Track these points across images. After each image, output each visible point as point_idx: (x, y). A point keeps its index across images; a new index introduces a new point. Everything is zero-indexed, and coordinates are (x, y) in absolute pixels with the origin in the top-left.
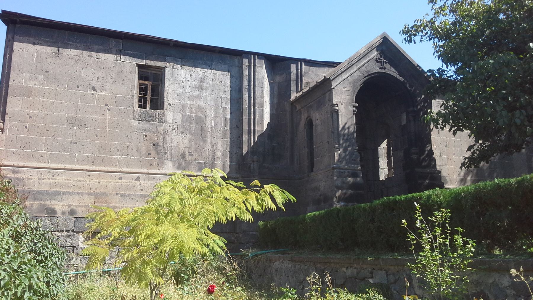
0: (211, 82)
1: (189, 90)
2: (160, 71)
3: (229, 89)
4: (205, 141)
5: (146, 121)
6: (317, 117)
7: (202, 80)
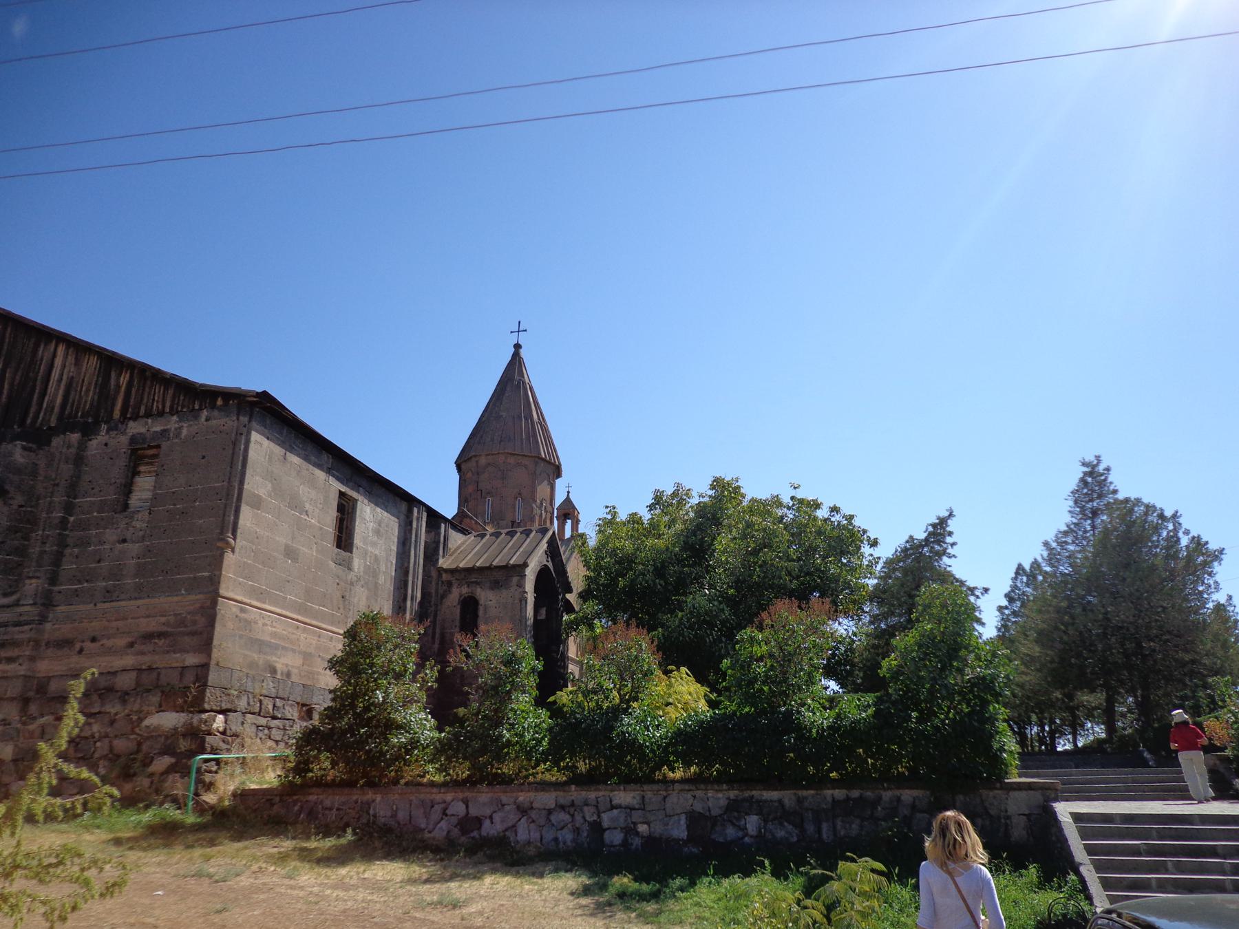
1: (370, 535)
3: (396, 540)
6: (487, 598)
7: (380, 525)
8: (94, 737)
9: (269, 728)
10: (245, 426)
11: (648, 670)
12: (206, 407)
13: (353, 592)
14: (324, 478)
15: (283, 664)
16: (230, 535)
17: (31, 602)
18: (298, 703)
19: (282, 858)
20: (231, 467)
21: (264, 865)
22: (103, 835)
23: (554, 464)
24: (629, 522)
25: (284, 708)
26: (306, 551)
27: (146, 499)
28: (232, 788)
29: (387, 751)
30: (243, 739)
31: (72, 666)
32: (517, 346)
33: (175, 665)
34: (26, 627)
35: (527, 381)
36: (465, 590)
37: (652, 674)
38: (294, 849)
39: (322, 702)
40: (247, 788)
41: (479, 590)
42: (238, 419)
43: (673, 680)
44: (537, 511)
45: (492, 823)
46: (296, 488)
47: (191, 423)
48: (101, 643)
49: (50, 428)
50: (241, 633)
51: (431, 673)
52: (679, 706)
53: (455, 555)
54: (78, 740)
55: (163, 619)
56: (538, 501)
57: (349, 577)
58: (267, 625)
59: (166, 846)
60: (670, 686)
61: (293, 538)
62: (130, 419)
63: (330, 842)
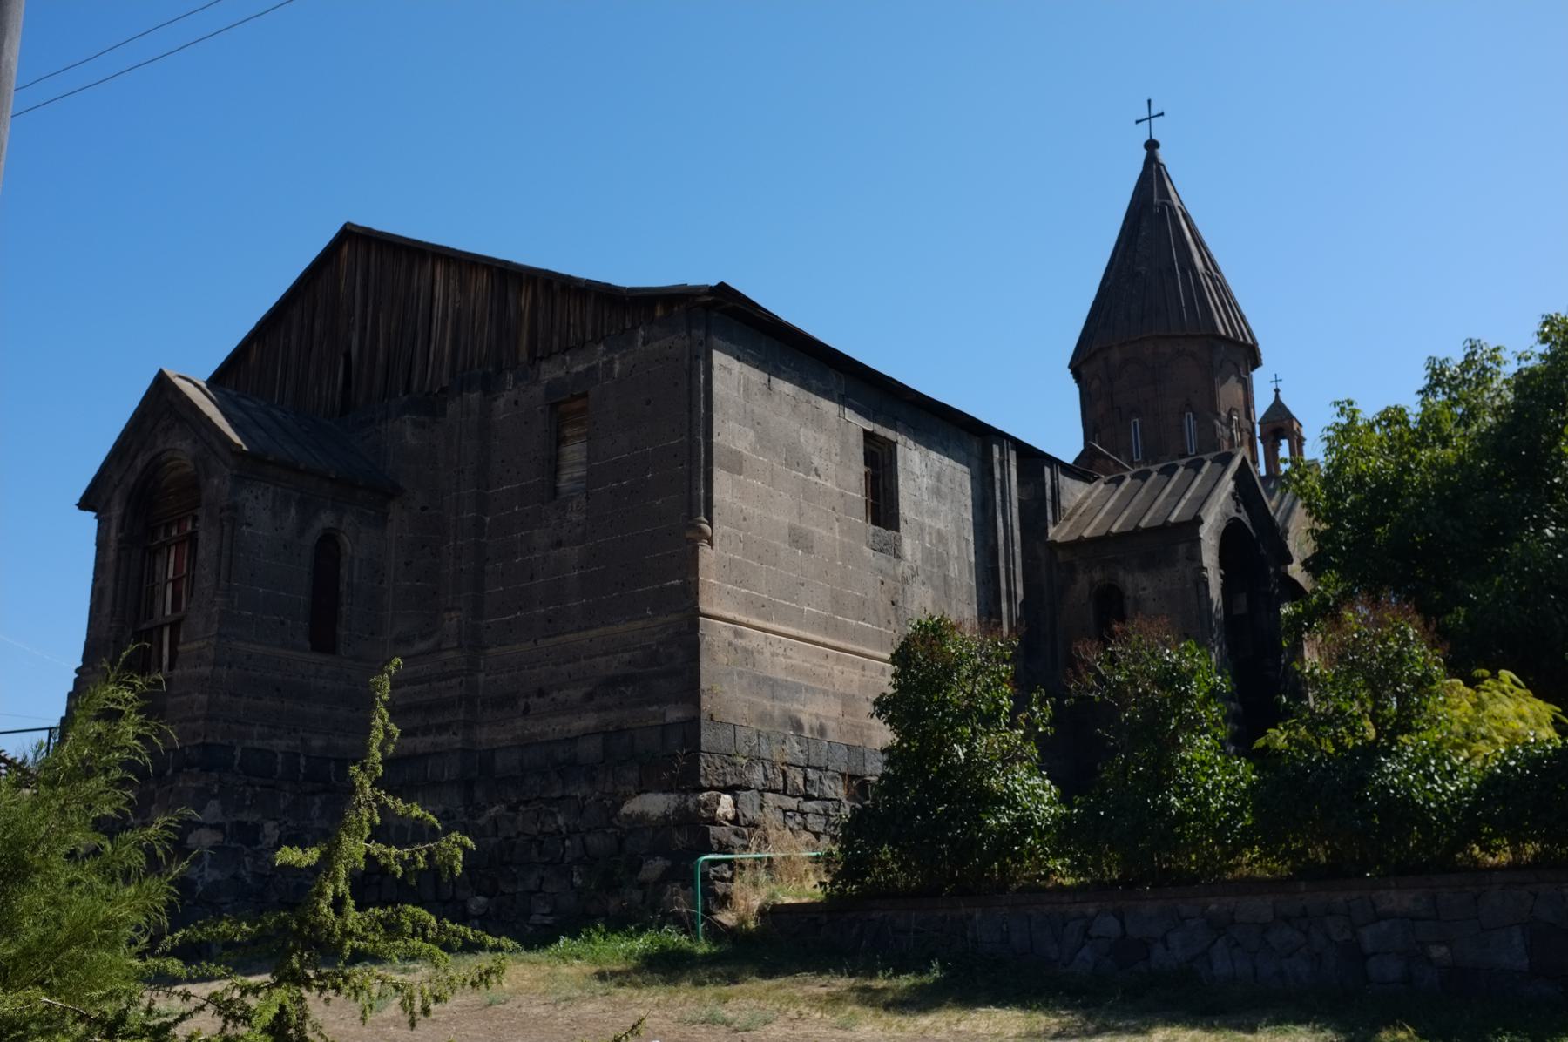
0: (950, 485)
1: (925, 497)
2: (879, 448)
3: (969, 502)
4: (950, 605)
5: (881, 551)
8: (561, 833)
9: (803, 814)
10: (701, 344)
11: (1424, 676)
12: (641, 323)
13: (909, 594)
14: (836, 414)
15: (811, 715)
16: (703, 518)
17: (455, 644)
18: (840, 774)
19: (836, 1000)
20: (690, 411)
21: (806, 1010)
22: (583, 968)
23: (1244, 345)
24: (1378, 422)
25: (821, 782)
26: (824, 533)
27: (580, 478)
28: (756, 903)
29: (983, 839)
30: (765, 830)
31: (519, 732)
32: (1152, 145)
33: (651, 723)
34: (455, 681)
35: (1176, 203)
36: (1097, 575)
37: (1433, 682)
38: (852, 990)
39: (874, 768)
40: (779, 903)
41: (1121, 573)
42: (689, 335)
43: (1484, 695)
44: (1223, 432)
45: (1167, 949)
46: (794, 434)
47: (624, 351)
48: (551, 697)
49: (442, 390)
50: (740, 668)
51: (1041, 712)
52: (1501, 739)
53: (1075, 517)
54: (540, 838)
55: (627, 656)
56: (1224, 414)
57: (899, 571)
58: (777, 655)
59: (667, 982)
60: (1479, 706)
61: (801, 515)
62: (541, 359)
63: (905, 981)
